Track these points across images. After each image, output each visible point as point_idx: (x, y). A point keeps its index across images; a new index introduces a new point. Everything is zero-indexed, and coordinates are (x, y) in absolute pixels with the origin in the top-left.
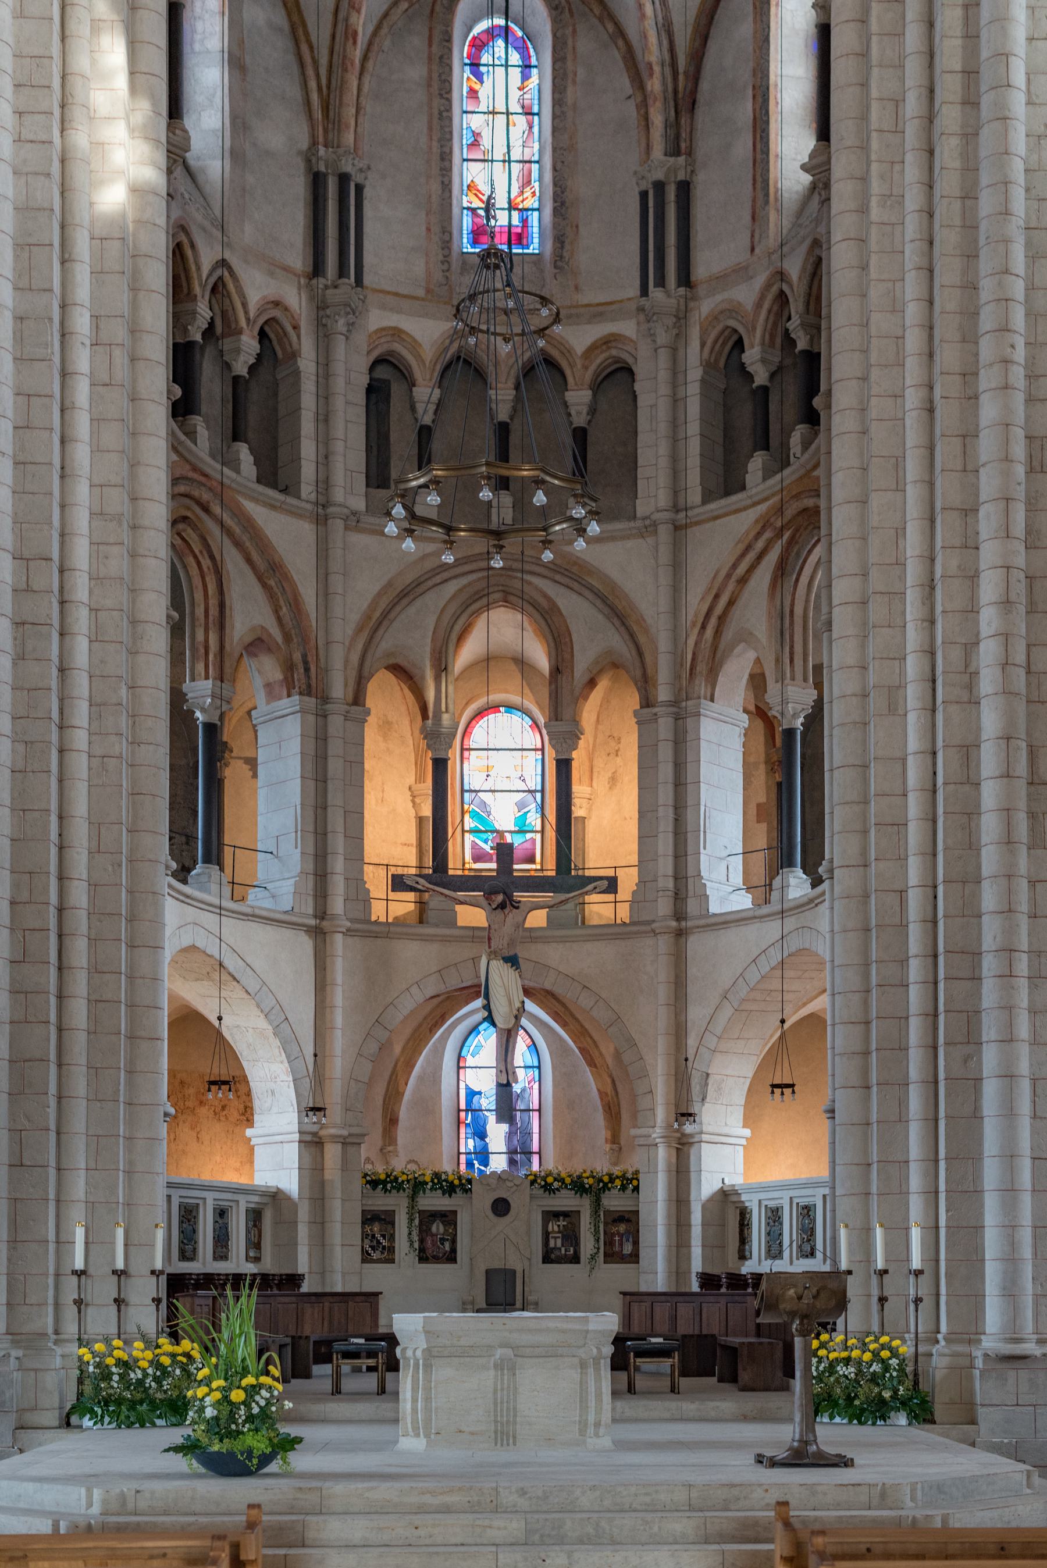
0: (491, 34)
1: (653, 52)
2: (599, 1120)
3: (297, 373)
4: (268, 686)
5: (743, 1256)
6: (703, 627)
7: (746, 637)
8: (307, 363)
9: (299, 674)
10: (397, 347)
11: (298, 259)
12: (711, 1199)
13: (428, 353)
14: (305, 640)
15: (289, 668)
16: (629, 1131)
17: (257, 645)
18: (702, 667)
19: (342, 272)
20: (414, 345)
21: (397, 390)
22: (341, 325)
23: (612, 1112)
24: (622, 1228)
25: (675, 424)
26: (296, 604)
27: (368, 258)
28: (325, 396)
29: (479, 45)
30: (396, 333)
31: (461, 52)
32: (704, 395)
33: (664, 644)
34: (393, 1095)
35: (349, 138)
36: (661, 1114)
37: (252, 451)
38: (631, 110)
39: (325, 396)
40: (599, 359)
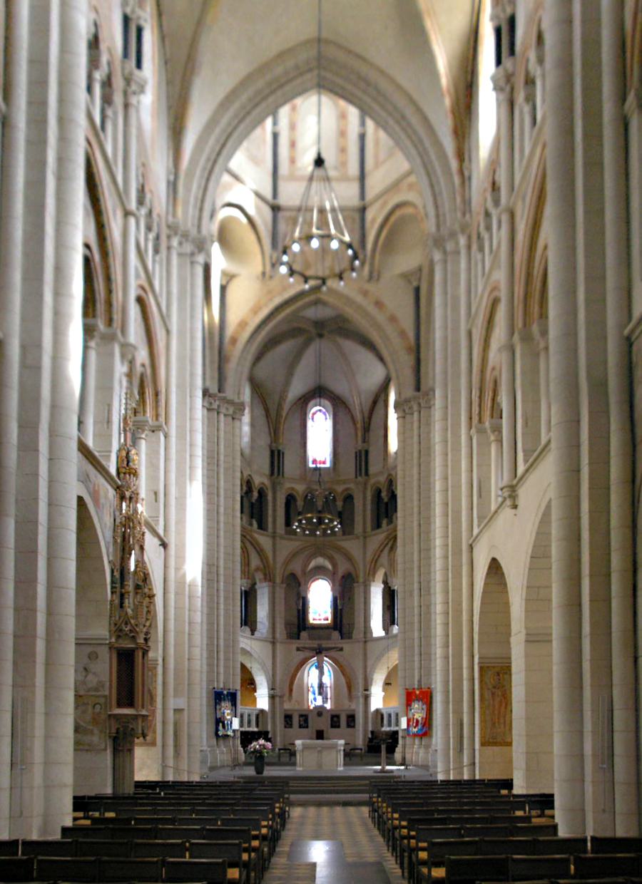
0: (316, 412)
1: (358, 416)
2: (345, 690)
3: (267, 500)
4: (260, 579)
5: (382, 726)
6: (372, 562)
7: (382, 565)
8: (270, 497)
9: (268, 577)
10: (295, 493)
11: (266, 468)
12: (374, 711)
13: (300, 493)
14: (269, 567)
15: (265, 575)
16: (353, 693)
17: (257, 569)
18: (371, 573)
19: (279, 474)
20: (297, 492)
21: (292, 502)
22: (278, 488)
23: (349, 688)
24: (351, 719)
25: (364, 511)
26: (267, 558)
27: (285, 470)
28: (274, 506)
29: (314, 414)
30: (293, 489)
31: (310, 416)
32: (372, 503)
33: (361, 567)
34: (292, 683)
35: (281, 441)
36: (361, 689)
37: (256, 521)
38: (353, 431)
39: (274, 506)
40: (346, 493)
